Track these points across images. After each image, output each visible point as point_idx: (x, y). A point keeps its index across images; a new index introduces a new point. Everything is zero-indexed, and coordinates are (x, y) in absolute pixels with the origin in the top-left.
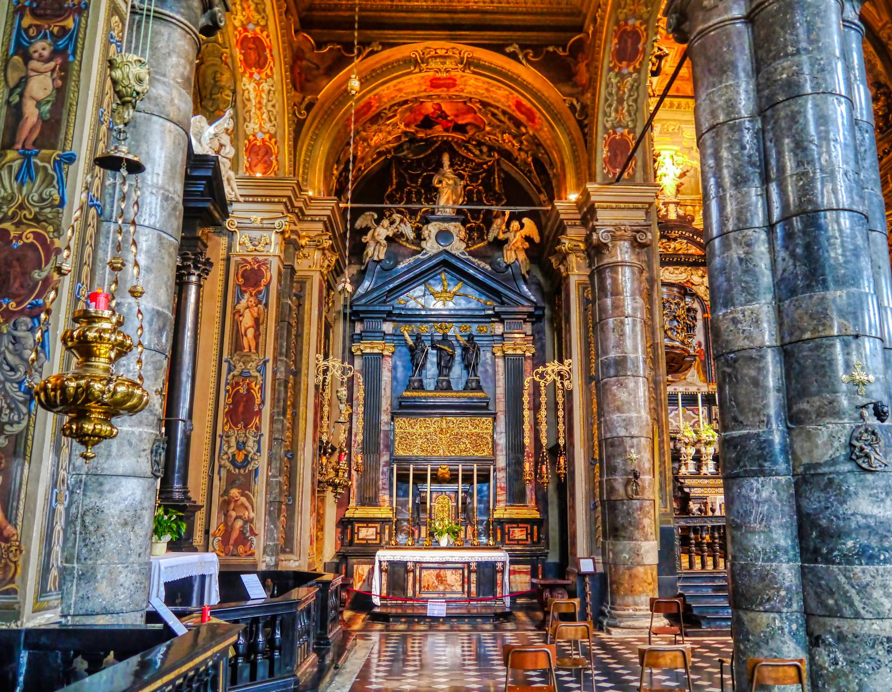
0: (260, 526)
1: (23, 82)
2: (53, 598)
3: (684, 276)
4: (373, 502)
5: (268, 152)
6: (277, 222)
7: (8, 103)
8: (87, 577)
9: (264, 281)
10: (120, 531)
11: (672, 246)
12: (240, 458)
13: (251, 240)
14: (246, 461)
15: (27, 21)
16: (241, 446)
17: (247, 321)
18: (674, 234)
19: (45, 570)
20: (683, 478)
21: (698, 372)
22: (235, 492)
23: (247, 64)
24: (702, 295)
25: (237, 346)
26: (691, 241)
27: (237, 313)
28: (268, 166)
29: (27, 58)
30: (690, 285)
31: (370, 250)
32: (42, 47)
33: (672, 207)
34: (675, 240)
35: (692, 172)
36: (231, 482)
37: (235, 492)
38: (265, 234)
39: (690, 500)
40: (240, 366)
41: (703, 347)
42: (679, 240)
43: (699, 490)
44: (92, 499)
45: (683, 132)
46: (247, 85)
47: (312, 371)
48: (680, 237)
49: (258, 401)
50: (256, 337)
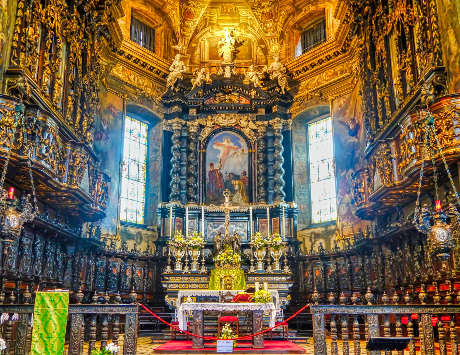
3: (234, 120)
11: (227, 98)
18: (228, 90)
20: (168, 276)
21: (242, 195)
24: (247, 135)
26: (241, 94)
30: (239, 128)
33: (228, 69)
34: (229, 93)
35: (247, 42)
39: (166, 294)
41: (247, 176)
42: (232, 93)
43: (175, 286)
48: (233, 91)
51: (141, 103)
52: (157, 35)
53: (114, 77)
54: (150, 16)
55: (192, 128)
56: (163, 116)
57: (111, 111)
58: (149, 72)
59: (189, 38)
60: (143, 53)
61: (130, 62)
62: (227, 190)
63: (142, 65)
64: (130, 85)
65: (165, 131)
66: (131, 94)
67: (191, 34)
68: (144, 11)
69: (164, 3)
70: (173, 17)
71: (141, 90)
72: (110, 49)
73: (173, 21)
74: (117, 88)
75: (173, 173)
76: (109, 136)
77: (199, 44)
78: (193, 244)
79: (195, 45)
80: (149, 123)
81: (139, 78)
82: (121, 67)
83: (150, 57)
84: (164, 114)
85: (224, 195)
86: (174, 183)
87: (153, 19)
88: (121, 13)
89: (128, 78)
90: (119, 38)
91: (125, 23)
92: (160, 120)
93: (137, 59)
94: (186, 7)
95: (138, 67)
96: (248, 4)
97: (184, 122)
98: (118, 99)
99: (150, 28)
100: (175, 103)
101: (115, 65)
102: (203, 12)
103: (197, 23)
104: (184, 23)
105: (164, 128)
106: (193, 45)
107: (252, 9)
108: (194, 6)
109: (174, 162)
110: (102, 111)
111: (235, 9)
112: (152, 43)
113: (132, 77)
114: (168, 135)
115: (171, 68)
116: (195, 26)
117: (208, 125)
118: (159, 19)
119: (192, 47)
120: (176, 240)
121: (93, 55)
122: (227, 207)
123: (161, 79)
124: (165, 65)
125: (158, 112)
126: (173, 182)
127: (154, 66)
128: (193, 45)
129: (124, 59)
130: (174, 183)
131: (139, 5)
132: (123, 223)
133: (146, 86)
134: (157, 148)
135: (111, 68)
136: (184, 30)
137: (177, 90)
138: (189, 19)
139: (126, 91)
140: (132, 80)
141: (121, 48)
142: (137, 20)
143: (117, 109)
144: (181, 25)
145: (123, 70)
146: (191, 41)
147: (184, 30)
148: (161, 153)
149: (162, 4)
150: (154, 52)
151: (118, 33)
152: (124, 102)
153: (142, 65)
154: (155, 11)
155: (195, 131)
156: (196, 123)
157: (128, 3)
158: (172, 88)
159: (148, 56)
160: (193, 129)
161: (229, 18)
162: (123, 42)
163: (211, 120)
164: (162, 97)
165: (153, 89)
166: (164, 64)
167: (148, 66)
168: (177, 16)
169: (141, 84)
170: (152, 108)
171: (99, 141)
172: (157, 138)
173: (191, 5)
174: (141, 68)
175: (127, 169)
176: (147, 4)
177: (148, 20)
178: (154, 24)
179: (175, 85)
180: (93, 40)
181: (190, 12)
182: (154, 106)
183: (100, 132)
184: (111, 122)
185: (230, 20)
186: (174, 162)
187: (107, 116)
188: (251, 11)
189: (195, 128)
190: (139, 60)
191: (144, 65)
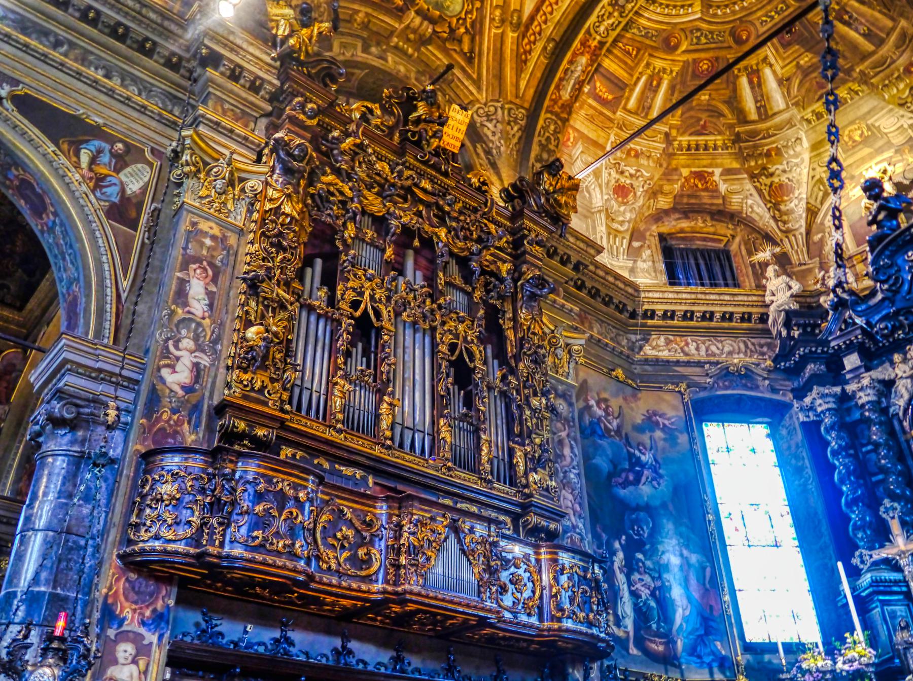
45: (878, 128)
51: (726, 388)
52: (735, 256)
53: (646, 361)
54: (705, 230)
55: (861, 394)
56: (791, 396)
57: (657, 423)
58: (726, 324)
59: (803, 230)
60: (693, 296)
61: (675, 322)
62: (887, 502)
63: (703, 318)
64: (688, 364)
65: (803, 423)
66: (696, 378)
67: (803, 222)
68: (688, 229)
69: (724, 198)
70: (753, 211)
71: (717, 363)
72: (624, 316)
73: (757, 218)
74: (660, 379)
75: (848, 504)
76: (661, 471)
77: (828, 230)
78: (846, 667)
79: (820, 236)
80: (769, 420)
81: (707, 343)
82: (662, 338)
83: (713, 297)
84: (792, 391)
85: (884, 516)
86: (856, 528)
87: (714, 234)
88: (593, 247)
89: (683, 351)
90: (630, 290)
91: (650, 263)
92: (789, 406)
93: (686, 312)
94: (768, 181)
95: (698, 324)
96: (889, 103)
97: (838, 389)
98: (668, 397)
99: (717, 252)
100: (805, 360)
101: (647, 340)
102: (805, 171)
103: (804, 196)
104: (779, 210)
105: (802, 417)
106: (816, 238)
107: (901, 105)
108: (784, 171)
109: (842, 481)
110: (627, 428)
111: (869, 129)
112: (728, 274)
113: (692, 348)
114: (811, 429)
115: (768, 299)
116: (803, 204)
117: (900, 374)
118: (724, 229)
119: (815, 243)
120: (805, 666)
121: (520, 335)
122: (903, 548)
123: (760, 326)
124: (755, 298)
125: (774, 390)
126: (855, 524)
127: (730, 309)
128: (816, 238)
129: (661, 322)
130: (856, 528)
131: (674, 223)
132: (749, 648)
133: (730, 353)
134: (800, 464)
135: (641, 348)
136: (785, 223)
137: (796, 333)
138: (785, 198)
139: (683, 377)
140: (694, 351)
141: (646, 307)
142: (686, 250)
143: (668, 416)
144: (774, 217)
145: (668, 342)
146: (808, 233)
147: (785, 223)
148: (810, 473)
149: (721, 201)
150: (736, 285)
151: (621, 285)
152: (683, 399)
153: (703, 318)
154: (712, 219)
155: (873, 398)
156: (866, 382)
157: (649, 229)
158: (784, 333)
159: (708, 297)
160: (864, 398)
161: (867, 151)
162: (643, 295)
163: (905, 360)
164: (773, 361)
165: (748, 352)
166: (750, 299)
167: (718, 315)
168: (759, 205)
169: (717, 352)
170: (756, 388)
171: (631, 488)
172: (793, 444)
173: (777, 172)
174: (705, 324)
175: (741, 527)
176: (690, 215)
177: (704, 239)
178: (720, 241)
179: (787, 324)
180: (515, 312)
181: (781, 186)
182: (760, 383)
183: (631, 470)
184: (661, 444)
185: (871, 153)
186: (842, 481)
187: (648, 434)
188: (902, 112)
189: (869, 391)
190: (692, 312)
191: (708, 316)
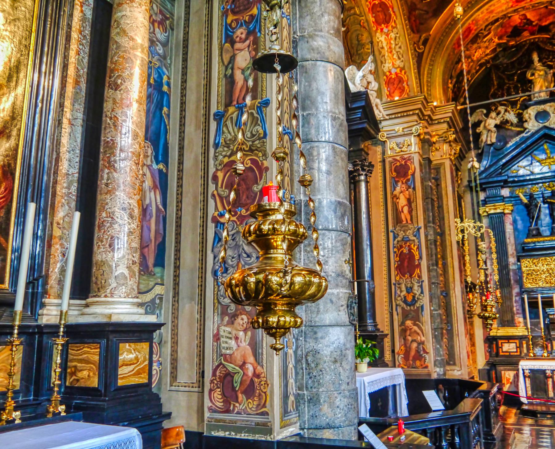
0: (430, 346)
1: (232, 59)
2: (293, 417)
4: (511, 323)
5: (401, 81)
6: (414, 129)
7: (225, 75)
8: (314, 401)
9: (410, 172)
10: (332, 367)
12: (410, 299)
13: (397, 145)
14: (414, 301)
15: (230, 18)
16: (409, 290)
17: (402, 201)
19: (285, 397)
22: (409, 323)
23: (378, 23)
25: (398, 220)
27: (395, 197)
28: (402, 90)
29: (233, 43)
31: (484, 138)
32: (241, 32)
36: (405, 316)
37: (409, 323)
38: (406, 138)
40: (401, 234)
44: (311, 344)
46: (381, 38)
47: (454, 232)
49: (417, 257)
50: (410, 212)
